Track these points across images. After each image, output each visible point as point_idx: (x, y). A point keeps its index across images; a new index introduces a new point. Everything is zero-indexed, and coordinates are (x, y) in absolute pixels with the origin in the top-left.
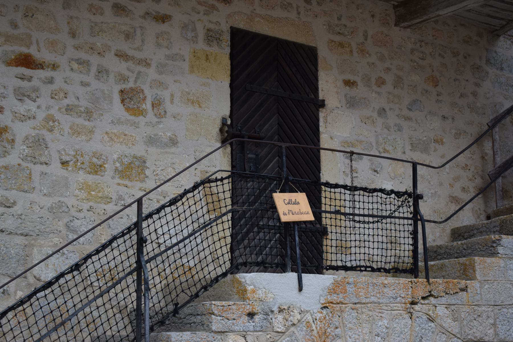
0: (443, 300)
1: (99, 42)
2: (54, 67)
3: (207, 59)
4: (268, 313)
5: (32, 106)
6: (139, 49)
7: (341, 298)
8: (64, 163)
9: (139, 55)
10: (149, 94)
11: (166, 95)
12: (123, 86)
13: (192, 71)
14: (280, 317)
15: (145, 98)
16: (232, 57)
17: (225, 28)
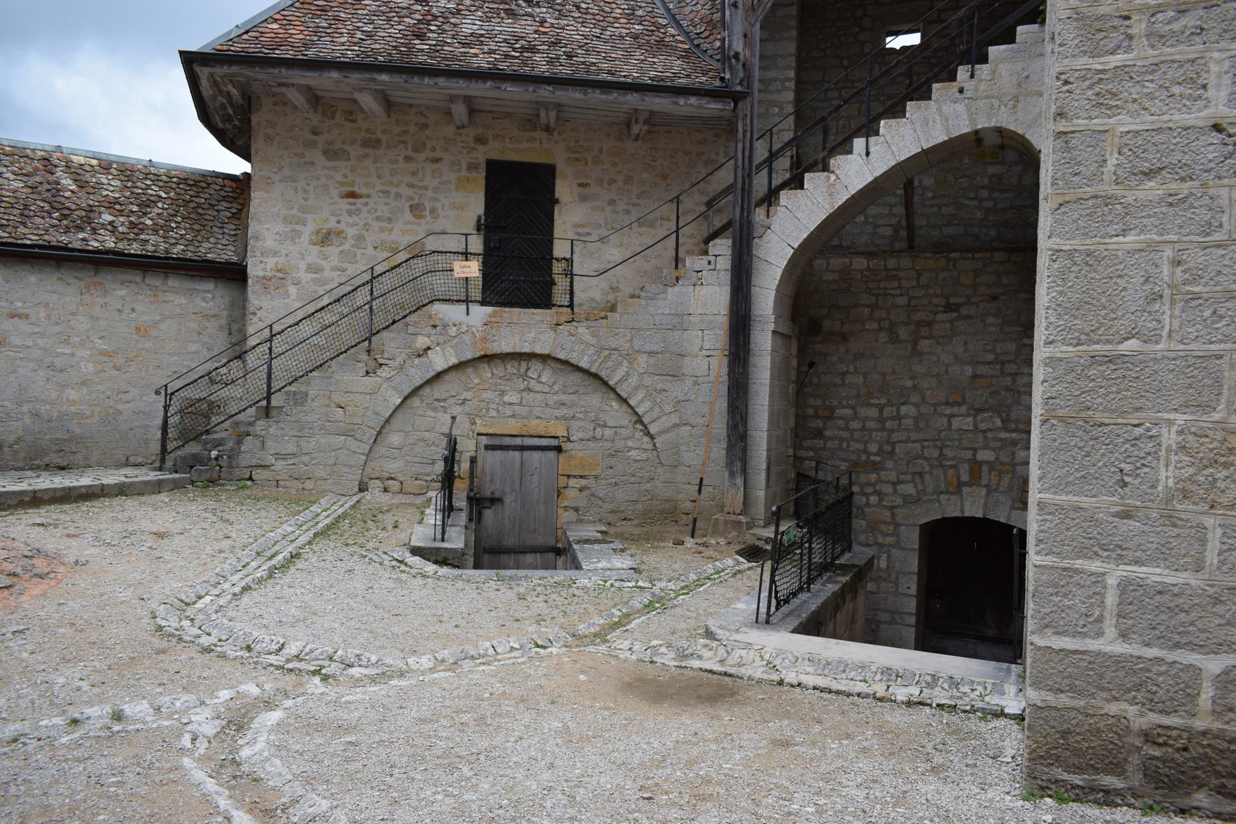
0: (584, 324)
1: (395, 180)
2: (368, 196)
3: (468, 181)
4: (445, 326)
5: (357, 219)
6: (421, 181)
7: (498, 319)
8: (375, 248)
9: (421, 184)
10: (428, 205)
11: (439, 205)
12: (411, 203)
13: (457, 189)
14: (454, 329)
15: (425, 209)
16: (487, 178)
17: (482, 160)
